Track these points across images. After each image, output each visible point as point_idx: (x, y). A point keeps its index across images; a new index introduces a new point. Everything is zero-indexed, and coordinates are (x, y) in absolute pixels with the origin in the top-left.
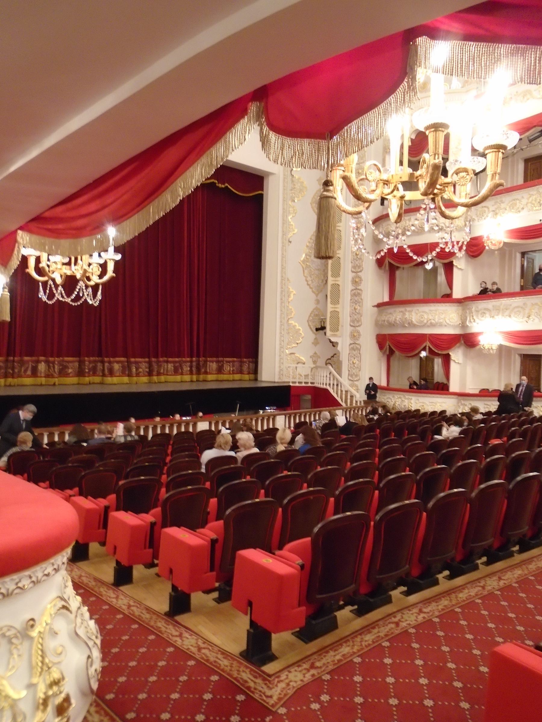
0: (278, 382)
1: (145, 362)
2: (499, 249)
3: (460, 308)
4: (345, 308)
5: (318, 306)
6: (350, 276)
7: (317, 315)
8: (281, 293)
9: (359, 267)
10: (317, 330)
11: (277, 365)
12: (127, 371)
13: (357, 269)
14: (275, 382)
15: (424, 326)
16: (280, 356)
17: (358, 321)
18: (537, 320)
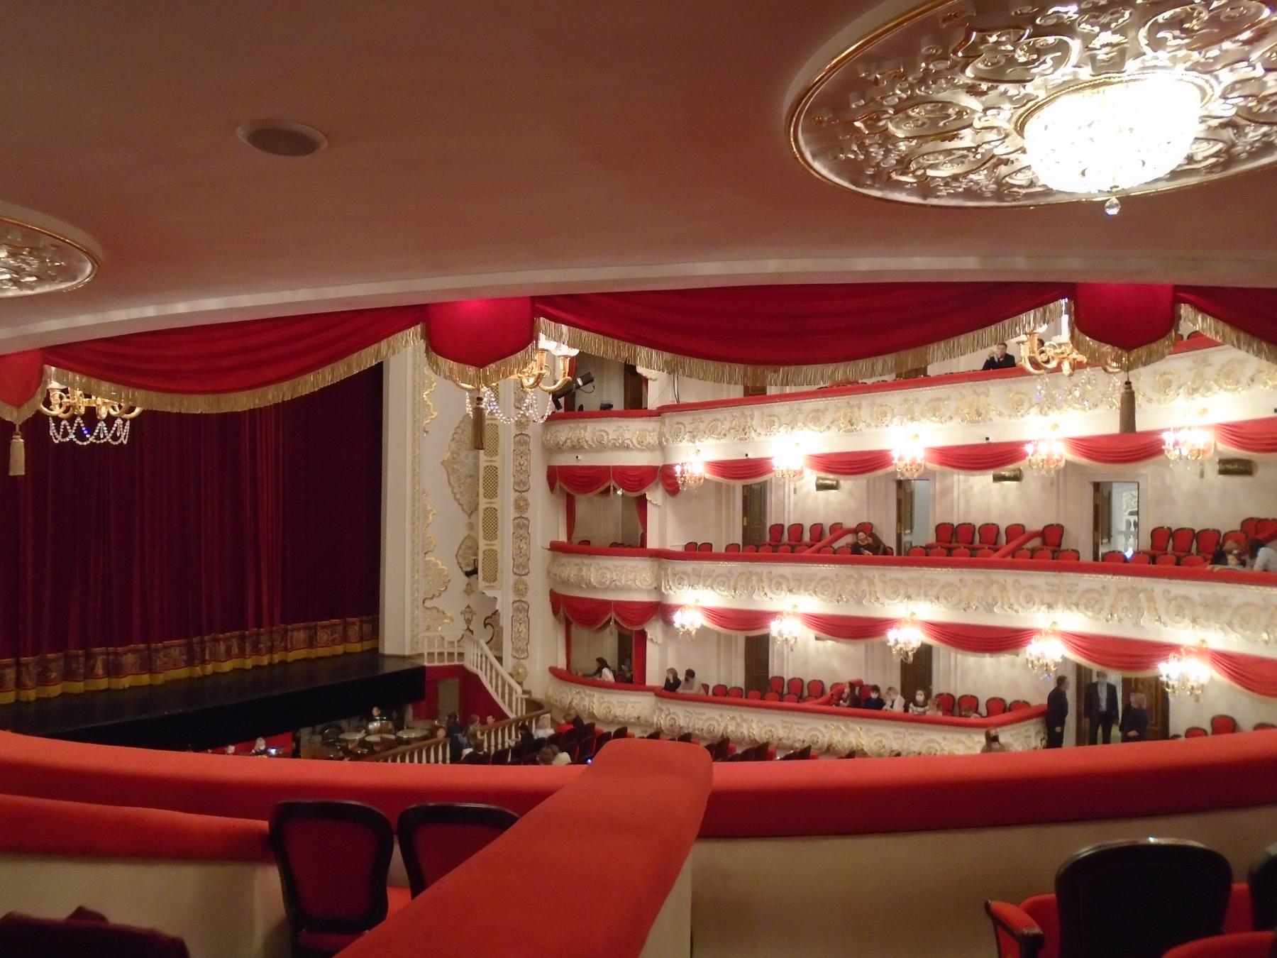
0: (409, 657)
1: (179, 646)
2: (699, 487)
3: (656, 564)
4: (505, 547)
5: (472, 533)
6: (513, 496)
7: (470, 548)
8: (413, 513)
9: (525, 484)
10: (468, 574)
11: (408, 629)
12: (147, 666)
13: (522, 486)
14: (403, 658)
15: (607, 589)
16: (413, 613)
17: (524, 567)
18: (744, 597)
